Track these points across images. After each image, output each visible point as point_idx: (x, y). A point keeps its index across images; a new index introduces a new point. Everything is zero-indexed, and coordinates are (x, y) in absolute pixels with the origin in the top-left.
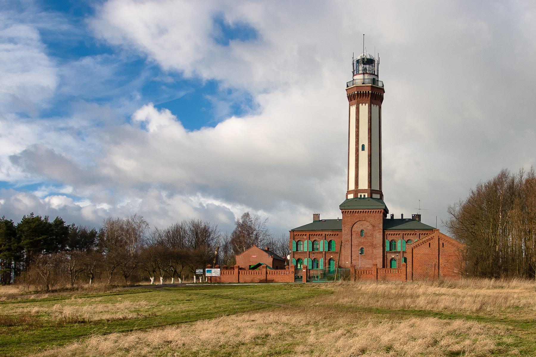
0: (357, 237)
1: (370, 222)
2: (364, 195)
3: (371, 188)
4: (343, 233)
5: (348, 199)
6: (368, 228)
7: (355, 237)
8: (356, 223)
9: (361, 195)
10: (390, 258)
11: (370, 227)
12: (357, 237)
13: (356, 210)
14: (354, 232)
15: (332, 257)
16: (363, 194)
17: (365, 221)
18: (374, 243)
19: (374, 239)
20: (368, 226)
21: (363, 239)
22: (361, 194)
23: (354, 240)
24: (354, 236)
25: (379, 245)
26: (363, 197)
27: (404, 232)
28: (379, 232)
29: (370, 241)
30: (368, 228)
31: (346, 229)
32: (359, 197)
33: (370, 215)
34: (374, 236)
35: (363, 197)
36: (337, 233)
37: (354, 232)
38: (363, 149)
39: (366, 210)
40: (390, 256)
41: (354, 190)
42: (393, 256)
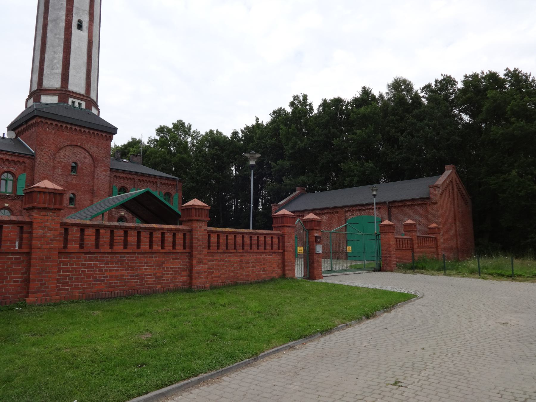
0: (64, 173)
1: (88, 152)
2: (80, 104)
3: (90, 95)
4: (37, 162)
5: (41, 103)
6: (86, 161)
7: (61, 173)
8: (64, 149)
9: (73, 102)
10: (117, 215)
11: (89, 160)
12: (64, 173)
13: (66, 125)
14: (59, 162)
15: (6, 205)
16: (77, 102)
17: (81, 147)
18: (95, 188)
19: (96, 181)
20: (85, 158)
21: (75, 178)
22: (74, 100)
23: (58, 177)
24: (59, 171)
25: (102, 193)
26: (77, 105)
27: (139, 178)
28: (104, 170)
29: (87, 183)
30: (86, 161)
31: (45, 155)
32: (70, 103)
33: (91, 139)
34: (96, 177)
35: (77, 105)
36: (22, 160)
37: (59, 163)
38: (80, 27)
39: (85, 129)
40: (118, 213)
41: (56, 90)
42: (123, 214)
